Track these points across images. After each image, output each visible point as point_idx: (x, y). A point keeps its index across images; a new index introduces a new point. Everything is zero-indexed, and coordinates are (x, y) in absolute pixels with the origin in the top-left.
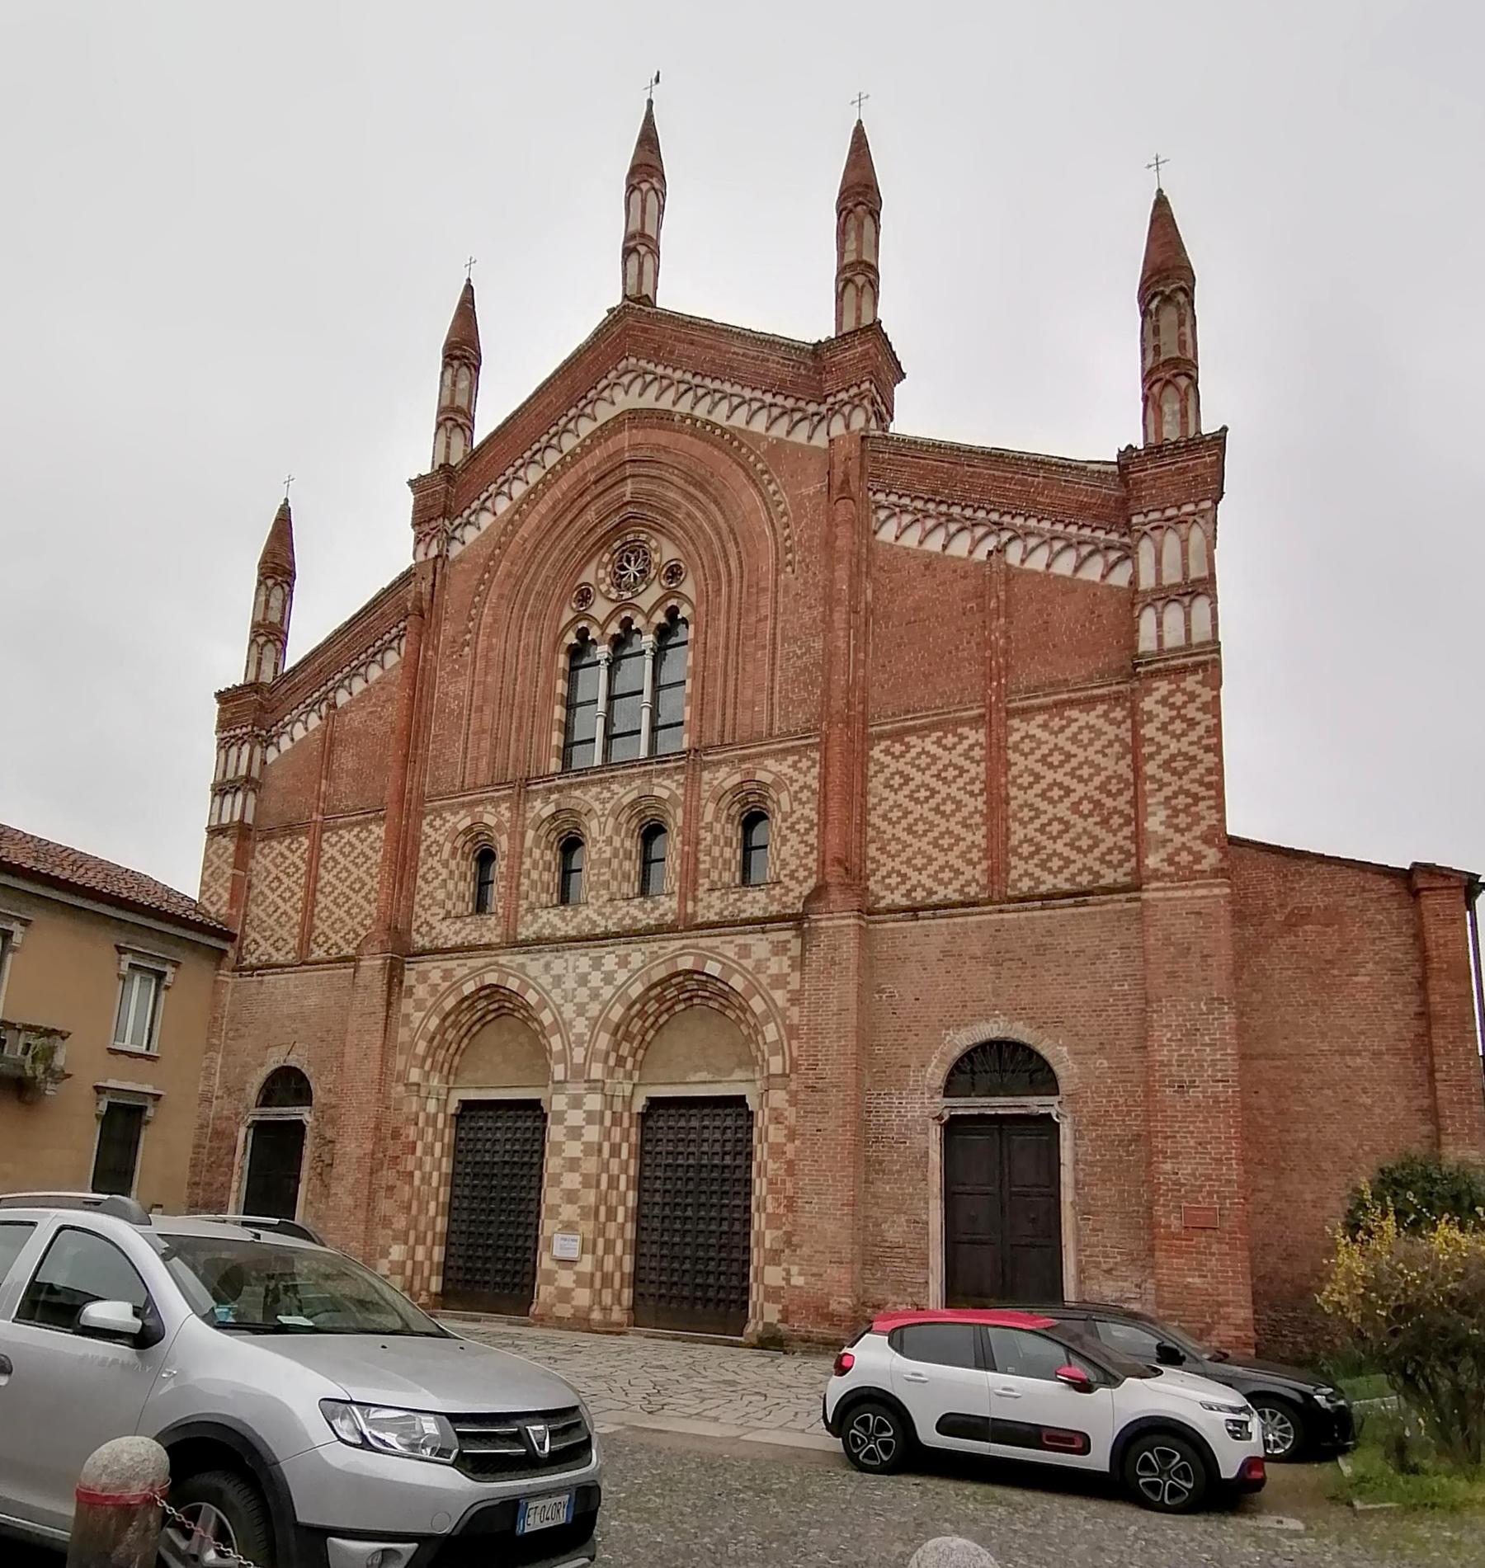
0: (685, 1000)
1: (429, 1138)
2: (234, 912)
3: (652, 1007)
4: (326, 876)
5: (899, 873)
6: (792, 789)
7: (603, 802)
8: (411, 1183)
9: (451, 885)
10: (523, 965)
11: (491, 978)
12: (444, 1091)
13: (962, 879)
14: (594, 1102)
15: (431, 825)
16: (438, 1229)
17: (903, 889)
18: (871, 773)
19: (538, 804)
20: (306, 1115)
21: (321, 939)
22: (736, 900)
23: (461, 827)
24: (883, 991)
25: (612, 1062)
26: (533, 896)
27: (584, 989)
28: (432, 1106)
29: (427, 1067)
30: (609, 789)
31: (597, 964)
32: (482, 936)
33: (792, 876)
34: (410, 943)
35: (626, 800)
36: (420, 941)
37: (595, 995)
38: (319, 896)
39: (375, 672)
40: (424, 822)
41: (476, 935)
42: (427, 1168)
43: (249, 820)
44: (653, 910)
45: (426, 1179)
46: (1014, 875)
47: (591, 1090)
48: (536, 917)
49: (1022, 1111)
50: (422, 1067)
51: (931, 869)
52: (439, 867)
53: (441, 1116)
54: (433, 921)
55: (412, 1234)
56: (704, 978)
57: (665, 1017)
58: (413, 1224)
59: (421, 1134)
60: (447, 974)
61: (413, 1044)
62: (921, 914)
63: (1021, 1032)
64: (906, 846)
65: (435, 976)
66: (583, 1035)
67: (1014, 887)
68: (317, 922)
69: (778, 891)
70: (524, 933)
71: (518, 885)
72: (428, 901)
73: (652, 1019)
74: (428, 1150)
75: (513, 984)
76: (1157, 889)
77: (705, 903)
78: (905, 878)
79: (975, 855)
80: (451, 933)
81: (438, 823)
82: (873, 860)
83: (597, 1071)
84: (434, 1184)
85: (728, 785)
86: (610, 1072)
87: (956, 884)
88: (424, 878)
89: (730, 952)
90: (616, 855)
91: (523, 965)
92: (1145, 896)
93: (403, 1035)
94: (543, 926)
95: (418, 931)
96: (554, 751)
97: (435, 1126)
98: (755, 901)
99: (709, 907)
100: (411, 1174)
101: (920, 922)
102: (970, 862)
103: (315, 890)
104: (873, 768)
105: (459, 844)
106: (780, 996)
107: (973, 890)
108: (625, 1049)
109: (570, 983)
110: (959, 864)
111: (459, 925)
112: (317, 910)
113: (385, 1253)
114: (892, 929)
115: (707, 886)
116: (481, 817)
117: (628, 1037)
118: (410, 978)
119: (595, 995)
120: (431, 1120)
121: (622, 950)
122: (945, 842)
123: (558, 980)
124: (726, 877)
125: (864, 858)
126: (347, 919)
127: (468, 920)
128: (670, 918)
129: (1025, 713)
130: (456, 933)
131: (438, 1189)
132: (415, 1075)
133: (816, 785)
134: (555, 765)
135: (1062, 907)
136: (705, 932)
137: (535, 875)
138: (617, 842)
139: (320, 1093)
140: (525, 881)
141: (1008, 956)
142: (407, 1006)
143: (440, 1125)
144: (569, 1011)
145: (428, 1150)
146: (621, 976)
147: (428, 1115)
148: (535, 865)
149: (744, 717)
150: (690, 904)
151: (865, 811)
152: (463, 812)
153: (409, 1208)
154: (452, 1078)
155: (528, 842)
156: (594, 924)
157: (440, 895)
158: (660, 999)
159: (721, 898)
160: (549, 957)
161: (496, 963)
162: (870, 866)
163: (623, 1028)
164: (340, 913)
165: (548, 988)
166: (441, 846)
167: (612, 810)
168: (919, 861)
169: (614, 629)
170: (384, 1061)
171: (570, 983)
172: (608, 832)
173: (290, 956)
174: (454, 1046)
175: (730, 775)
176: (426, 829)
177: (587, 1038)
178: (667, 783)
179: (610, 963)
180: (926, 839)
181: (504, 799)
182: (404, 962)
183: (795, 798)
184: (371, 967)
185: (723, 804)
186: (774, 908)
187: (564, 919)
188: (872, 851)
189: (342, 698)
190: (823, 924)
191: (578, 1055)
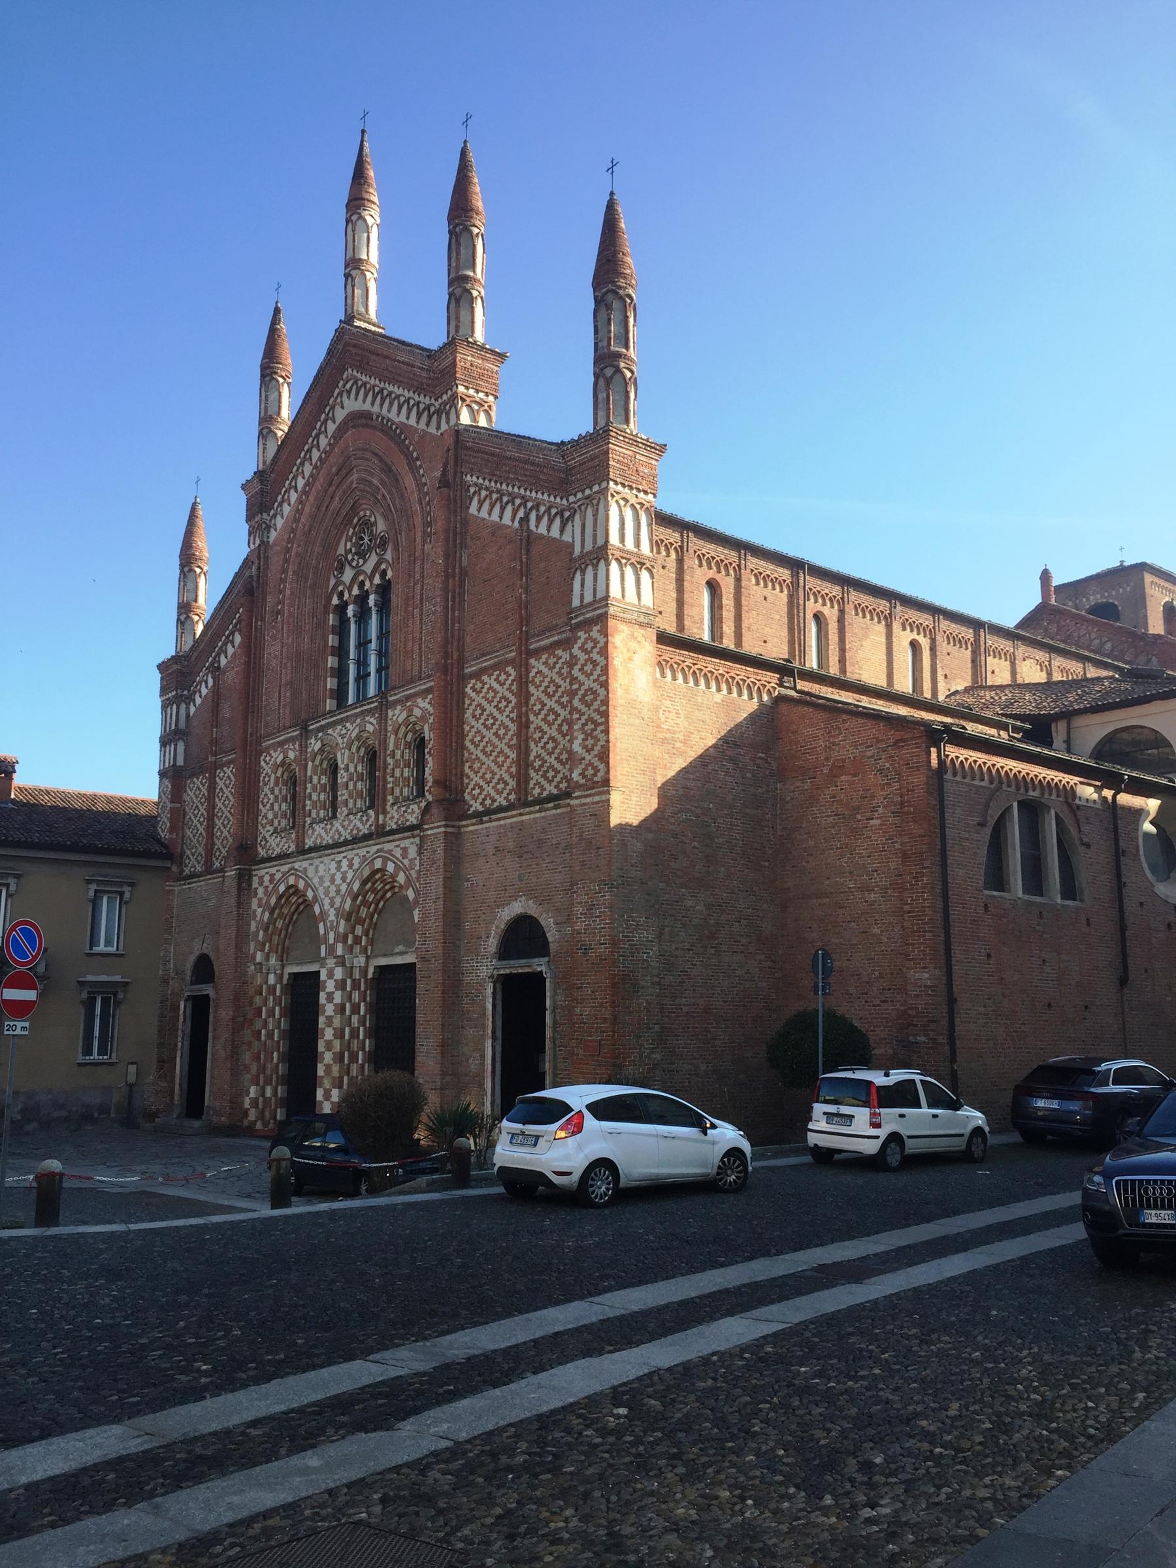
2: (174, 836)
3: (371, 897)
9: (276, 807)
10: (305, 869)
11: (292, 880)
12: (278, 967)
14: (339, 973)
24: (468, 880)
26: (314, 815)
28: (272, 979)
34: (257, 853)
36: (262, 852)
37: (338, 891)
43: (180, 762)
45: (270, 1035)
46: (532, 783)
47: (337, 964)
49: (527, 970)
52: (269, 793)
55: (262, 1078)
57: (382, 903)
58: (262, 1069)
61: (257, 933)
62: (485, 819)
63: (533, 909)
66: (332, 922)
70: (309, 843)
72: (264, 821)
74: (271, 1013)
76: (577, 798)
81: (268, 759)
85: (400, 720)
86: (350, 950)
89: (398, 853)
90: (351, 779)
91: (305, 869)
92: (573, 802)
98: (413, 812)
100: (259, 1032)
103: (214, 815)
105: (279, 774)
108: (359, 930)
113: (248, 1093)
117: (360, 921)
120: (272, 990)
121: (350, 855)
124: (406, 790)
129: (537, 653)
132: (259, 957)
134: (330, 704)
135: (549, 809)
137: (315, 797)
138: (352, 769)
140: (308, 802)
141: (525, 849)
145: (271, 1013)
147: (269, 987)
148: (314, 789)
150: (381, 817)
151: (462, 736)
153: (258, 1058)
155: (309, 774)
158: (373, 890)
160: (317, 862)
162: (466, 781)
169: (356, 591)
170: (239, 948)
179: (345, 863)
182: (251, 870)
185: (401, 735)
190: (429, 832)
191: (331, 936)
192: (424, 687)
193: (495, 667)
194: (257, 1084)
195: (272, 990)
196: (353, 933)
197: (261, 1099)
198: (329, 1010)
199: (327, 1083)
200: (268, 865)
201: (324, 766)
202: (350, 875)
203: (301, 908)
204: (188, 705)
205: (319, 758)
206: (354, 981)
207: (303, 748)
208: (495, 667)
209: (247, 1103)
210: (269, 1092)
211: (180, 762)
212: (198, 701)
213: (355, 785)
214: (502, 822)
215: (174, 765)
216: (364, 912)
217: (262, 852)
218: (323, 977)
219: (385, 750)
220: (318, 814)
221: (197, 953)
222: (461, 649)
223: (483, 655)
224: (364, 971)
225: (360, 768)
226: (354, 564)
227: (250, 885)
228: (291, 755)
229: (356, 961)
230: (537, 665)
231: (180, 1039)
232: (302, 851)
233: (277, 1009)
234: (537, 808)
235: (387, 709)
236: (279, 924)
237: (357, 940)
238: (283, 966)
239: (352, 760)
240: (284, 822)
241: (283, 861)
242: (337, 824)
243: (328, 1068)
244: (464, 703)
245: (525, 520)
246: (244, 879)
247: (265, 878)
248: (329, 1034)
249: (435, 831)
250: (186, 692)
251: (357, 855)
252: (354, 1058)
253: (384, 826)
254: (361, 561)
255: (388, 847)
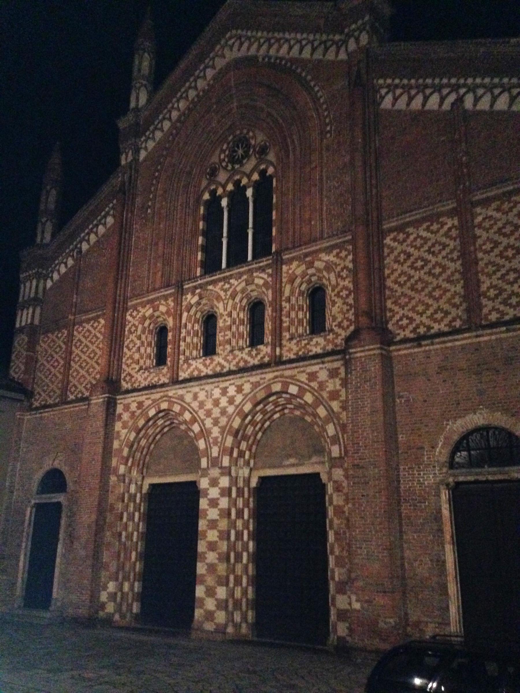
0: (279, 411)
1: (131, 509)
4: (76, 351)
5: (408, 318)
6: (337, 271)
7: (225, 291)
8: (120, 541)
9: (142, 350)
11: (164, 406)
12: (140, 479)
13: (450, 317)
14: (225, 482)
15: (131, 315)
16: (137, 570)
17: (411, 327)
18: (386, 254)
19: (189, 296)
20: (61, 498)
21: (73, 389)
22: (306, 345)
23: (147, 315)
25: (235, 454)
26: (187, 353)
27: (217, 408)
28: (133, 489)
29: (130, 464)
30: (229, 283)
31: (224, 391)
32: (159, 379)
33: (339, 325)
34: (120, 386)
35: (238, 289)
37: (223, 412)
38: (72, 363)
39: (101, 229)
40: (128, 314)
41: (156, 379)
42: (130, 529)
44: (256, 355)
45: (129, 537)
47: (222, 474)
48: (189, 365)
50: (126, 464)
51: (429, 313)
52: (135, 339)
53: (138, 495)
54: (133, 373)
56: (288, 396)
57: (268, 423)
59: (127, 506)
60: (140, 405)
61: (121, 450)
62: (423, 343)
64: (411, 298)
65: (133, 407)
66: (216, 439)
67: (486, 319)
68: (71, 378)
69: (331, 336)
70: (183, 375)
71: (179, 346)
72: (130, 361)
73: (259, 426)
74: (131, 517)
75: (177, 408)
77: (287, 348)
78: (411, 320)
79: (457, 300)
80: (142, 379)
81: (135, 314)
82: (391, 310)
83: (226, 461)
84: (135, 539)
86: (234, 462)
87: (446, 321)
88: (127, 347)
89: (303, 378)
93: (116, 444)
94: (194, 371)
95: (124, 380)
96: (199, 264)
97: (135, 501)
98: (317, 344)
99: (290, 350)
100: (120, 535)
101: (423, 349)
102: (455, 306)
103: (70, 360)
104: (386, 251)
106: (335, 405)
107: (458, 324)
108: (244, 445)
109: (209, 405)
110: (446, 307)
111: (147, 373)
112: (71, 372)
113: (105, 588)
114: (405, 355)
115: (288, 337)
116: (158, 307)
117: (245, 438)
118: (119, 409)
119: (223, 412)
120: (132, 498)
122: (437, 294)
123: (202, 405)
124: (300, 330)
125: (383, 309)
126: (87, 376)
127: (152, 371)
128: (266, 359)
130: (145, 379)
131: (137, 543)
132: (122, 469)
133: (351, 266)
136: (288, 366)
137: (188, 339)
138: (234, 315)
139: (71, 484)
140: (182, 344)
142: (118, 426)
143: (138, 501)
144: (209, 422)
145: (131, 517)
146: (239, 399)
148: (188, 333)
149: (306, 230)
150: (278, 350)
151: (383, 279)
152: (148, 306)
154: (145, 470)
155: (184, 321)
156: (223, 367)
157: (137, 356)
158: (264, 412)
159: (297, 344)
161: (166, 396)
162: (388, 314)
163: (241, 432)
164: (83, 372)
165: (196, 409)
166: (137, 327)
167: (231, 295)
168: (420, 308)
171: (209, 405)
172: (229, 309)
173: (57, 401)
174: (145, 450)
175: (299, 266)
176: (128, 318)
177: (219, 440)
178: (262, 275)
180: (423, 294)
181: (170, 295)
182: (116, 399)
183: (339, 276)
184: (96, 404)
186: (330, 347)
187: (205, 365)
188: (389, 304)
189: (85, 247)
190: (358, 355)
192: (328, 244)
193: (424, 220)
194: (117, 579)
195: (132, 498)
196: (238, 447)
197: (119, 594)
198: (213, 514)
199: (210, 581)
200: (135, 394)
201: (198, 316)
202: (239, 399)
203: (166, 430)
204: (46, 280)
205: (194, 309)
206: (238, 489)
207: (178, 303)
208: (424, 220)
209: (104, 597)
210: (126, 587)
211: (36, 322)
212: (56, 276)
213: (238, 329)
214: (449, 345)
215: (32, 323)
216: (250, 430)
217: (125, 385)
218: (204, 483)
219: (281, 297)
220: (191, 353)
221: (46, 468)
222: (379, 209)
223: (407, 212)
224: (247, 481)
225: (241, 315)
226: (230, 167)
227: (115, 411)
228: (163, 309)
229: (241, 472)
230: (481, 214)
231: (24, 539)
232: (175, 381)
233: (137, 514)
234: (504, 328)
235: (282, 265)
236: (143, 442)
237: (241, 454)
238: (143, 478)
239: (235, 308)
240: (148, 362)
241: (153, 391)
242: (218, 359)
243: (212, 568)
244: (383, 251)
245: (460, 100)
246: (110, 406)
247: (128, 405)
248: (212, 535)
249: (372, 353)
250: (44, 272)
251: (247, 383)
252: (238, 558)
253: (281, 356)
254: (237, 166)
255: (288, 373)
